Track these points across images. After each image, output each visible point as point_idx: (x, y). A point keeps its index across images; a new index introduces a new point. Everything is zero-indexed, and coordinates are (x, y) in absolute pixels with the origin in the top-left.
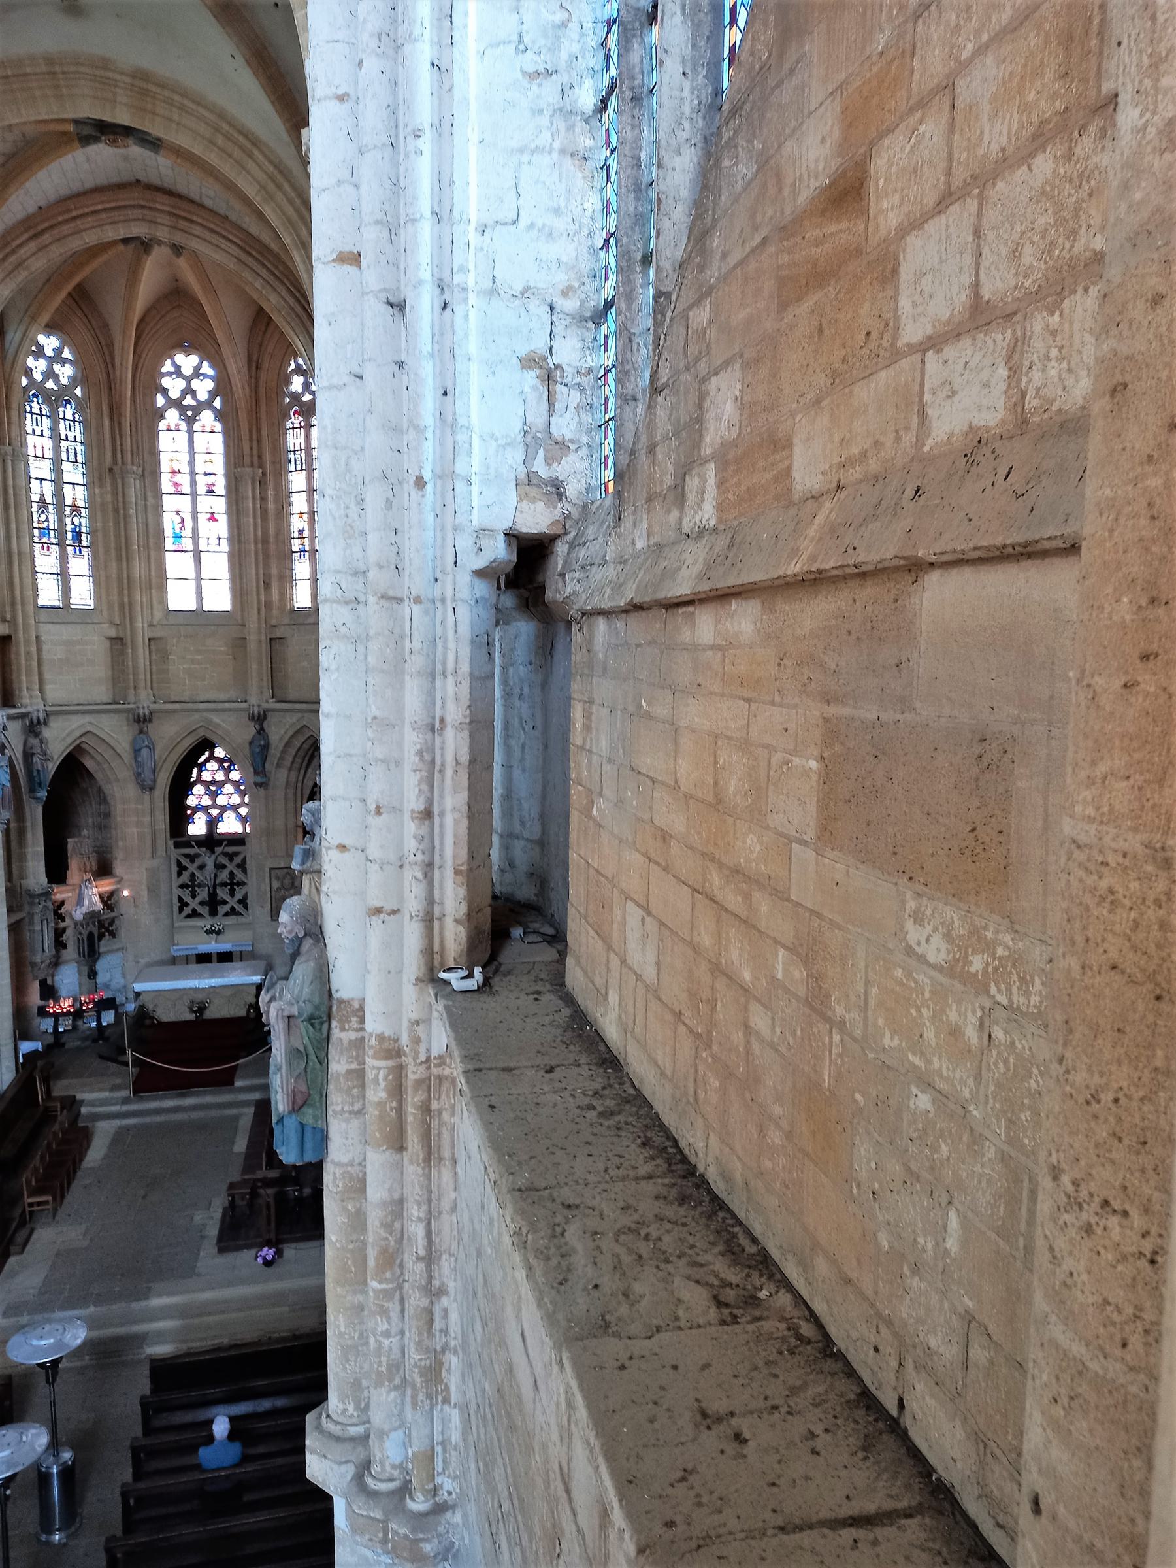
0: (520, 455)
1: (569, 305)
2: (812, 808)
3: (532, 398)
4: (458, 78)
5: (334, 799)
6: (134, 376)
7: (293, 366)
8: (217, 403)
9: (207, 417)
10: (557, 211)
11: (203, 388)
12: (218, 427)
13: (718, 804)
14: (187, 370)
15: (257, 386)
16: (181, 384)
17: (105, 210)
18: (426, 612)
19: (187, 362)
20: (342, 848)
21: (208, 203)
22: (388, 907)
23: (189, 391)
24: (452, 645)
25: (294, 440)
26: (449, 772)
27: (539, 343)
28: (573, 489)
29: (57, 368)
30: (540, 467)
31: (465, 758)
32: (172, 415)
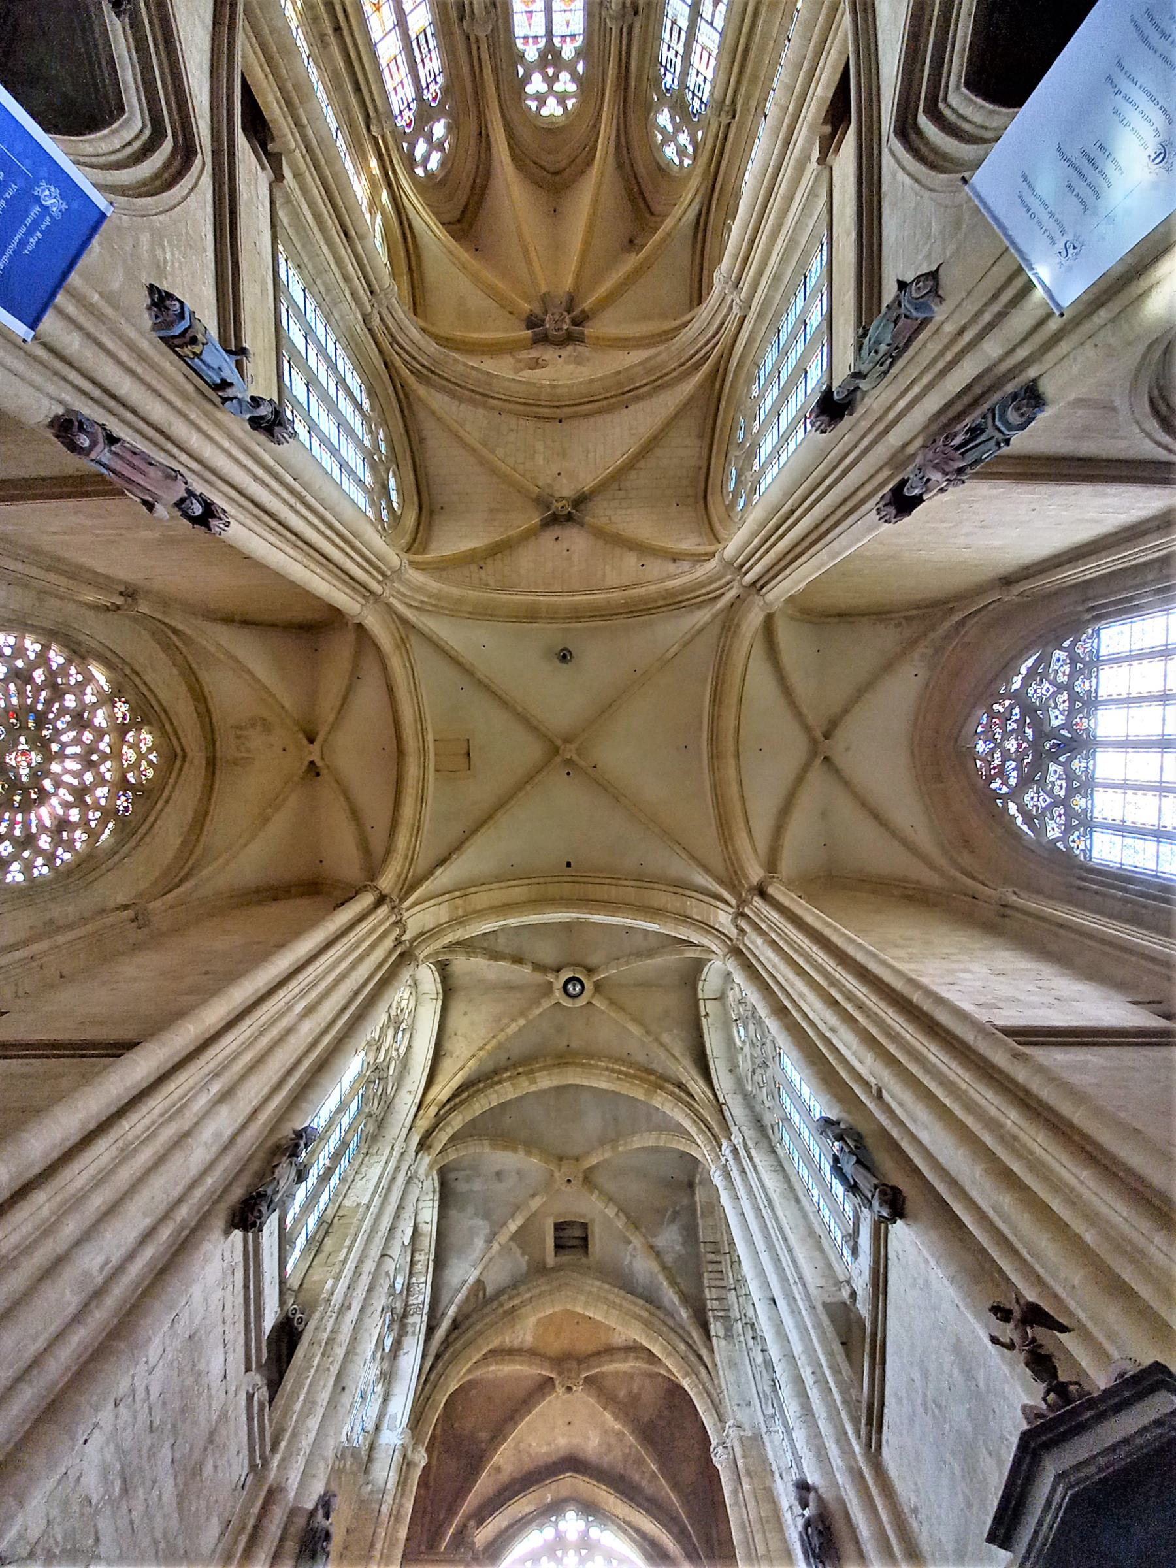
6: (601, 108)
7: (446, 145)
8: (521, 71)
9: (531, 53)
11: (536, 85)
12: (519, 43)
14: (551, 101)
15: (479, 118)
16: (558, 87)
17: (583, 404)
19: (552, 108)
21: (513, 422)
23: (551, 81)
25: (432, 64)
29: (670, 129)
32: (568, 52)
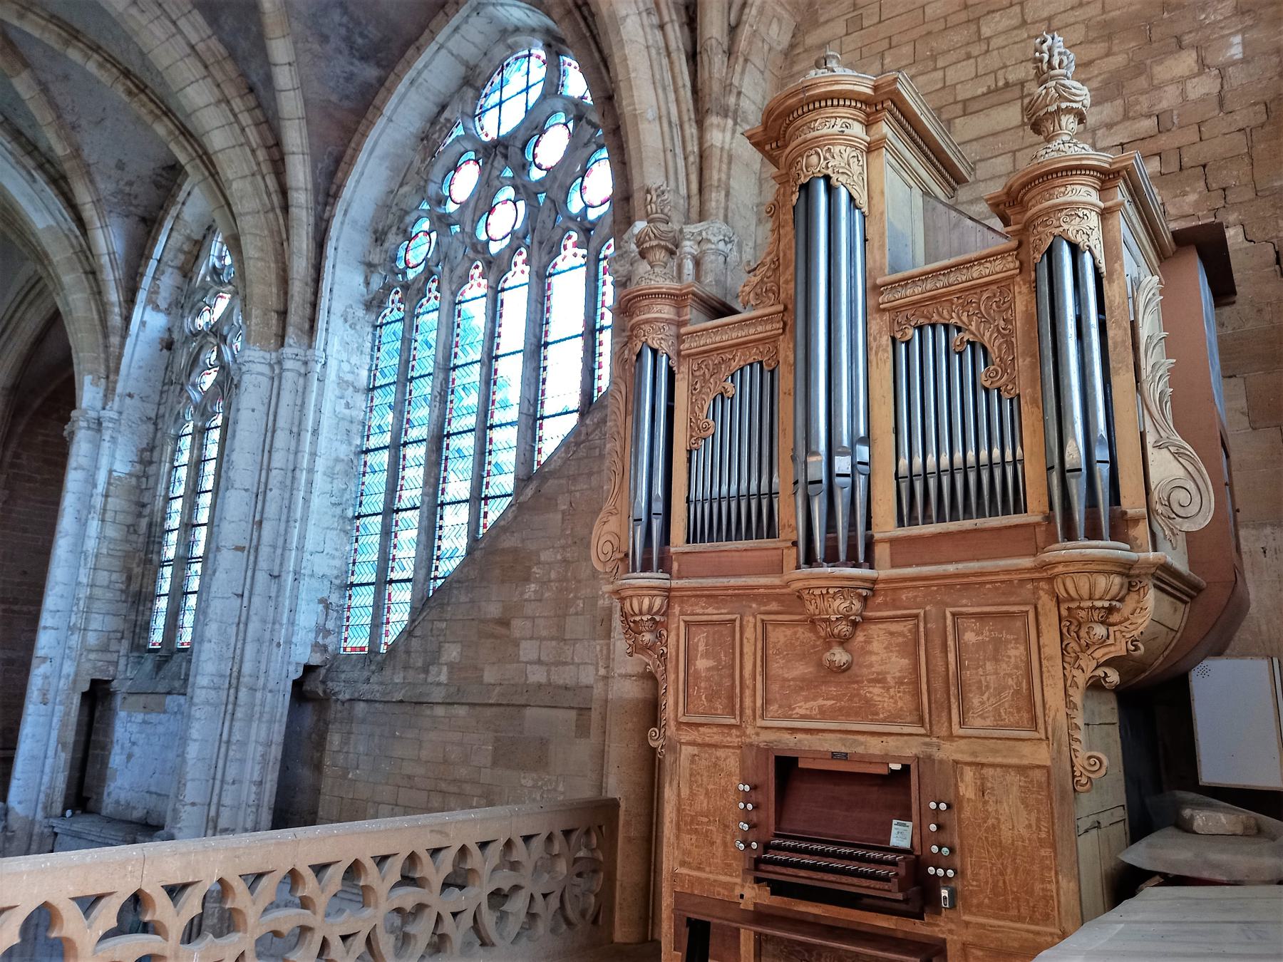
0: (314, 635)
1: (337, 582)
2: (489, 758)
3: (320, 614)
4: (312, 504)
5: (193, 780)
10: (336, 549)
13: (446, 761)
18: (274, 696)
20: (193, 804)
22: (232, 827)
24: (279, 709)
26: (271, 764)
27: (325, 595)
28: (330, 649)
30: (320, 640)
31: (279, 757)
